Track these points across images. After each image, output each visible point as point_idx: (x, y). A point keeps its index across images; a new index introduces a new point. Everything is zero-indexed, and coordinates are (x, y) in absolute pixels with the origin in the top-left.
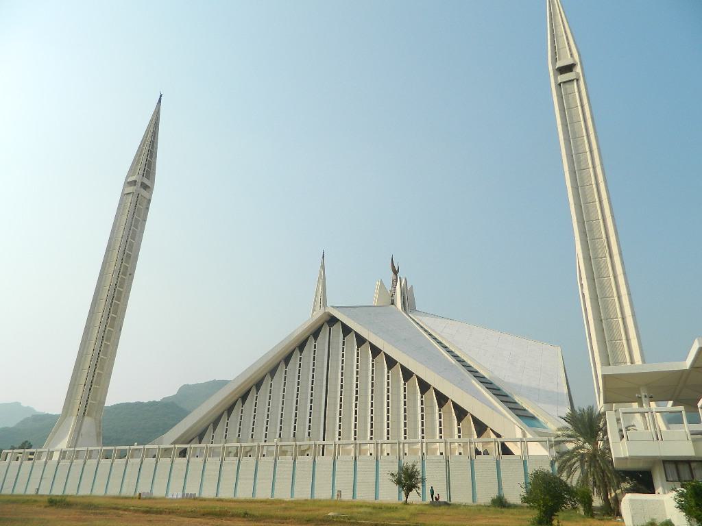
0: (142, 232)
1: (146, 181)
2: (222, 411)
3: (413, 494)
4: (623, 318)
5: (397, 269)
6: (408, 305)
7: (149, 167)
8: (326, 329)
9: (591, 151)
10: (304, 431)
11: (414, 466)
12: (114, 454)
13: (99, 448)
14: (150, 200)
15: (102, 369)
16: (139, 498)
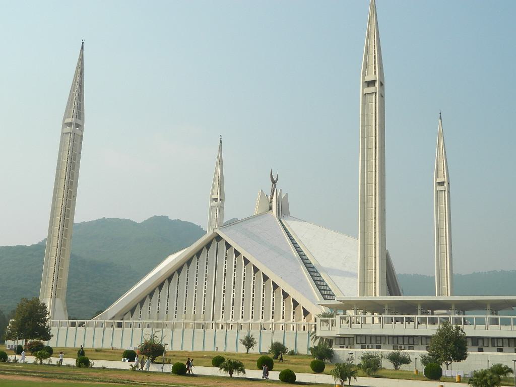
0: (79, 163)
1: (79, 122)
2: (146, 295)
3: (251, 349)
4: (375, 257)
5: (275, 179)
6: (283, 211)
7: (80, 109)
8: (215, 243)
9: (376, 148)
10: (201, 311)
11: (252, 336)
12: (77, 325)
13: (67, 321)
14: (82, 136)
15: (62, 266)
16: (113, 349)
